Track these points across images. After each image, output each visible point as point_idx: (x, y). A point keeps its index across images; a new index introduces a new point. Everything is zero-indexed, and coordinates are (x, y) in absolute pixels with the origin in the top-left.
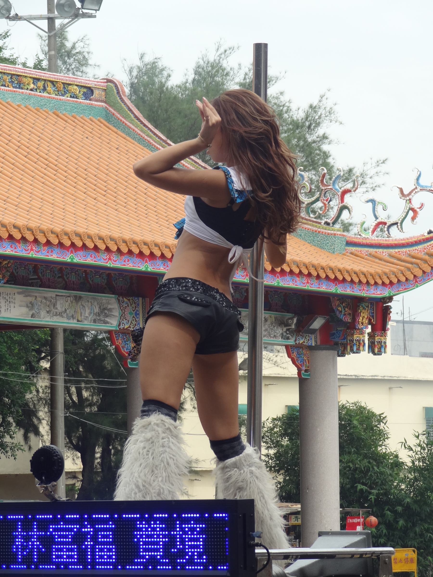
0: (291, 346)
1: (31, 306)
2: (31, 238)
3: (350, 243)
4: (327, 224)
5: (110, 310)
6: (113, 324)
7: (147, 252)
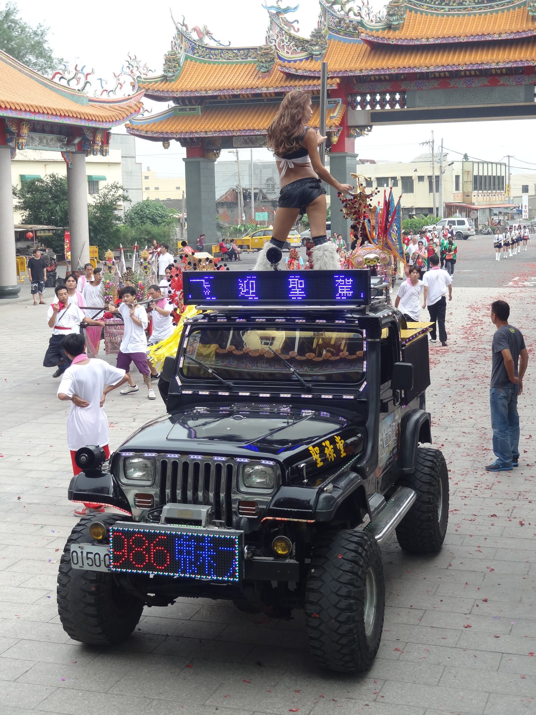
0: (64, 152)
3: (90, 101)
4: (79, 90)
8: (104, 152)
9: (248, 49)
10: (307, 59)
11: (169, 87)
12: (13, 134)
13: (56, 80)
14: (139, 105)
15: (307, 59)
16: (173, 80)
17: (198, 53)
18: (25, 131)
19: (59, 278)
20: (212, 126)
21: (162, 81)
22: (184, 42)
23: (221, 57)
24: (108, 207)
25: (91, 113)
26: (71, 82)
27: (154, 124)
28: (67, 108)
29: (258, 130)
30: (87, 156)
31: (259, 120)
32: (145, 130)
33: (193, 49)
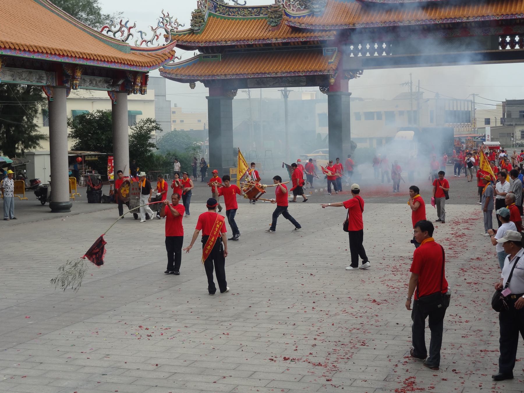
1: (12, 76)
2: (18, 48)
3: (132, 49)
4: (123, 41)
5: (43, 77)
6: (44, 83)
7: (62, 54)
8: (143, 92)
9: (261, 8)
10: (309, 15)
11: (196, 38)
12: (69, 76)
13: (104, 32)
14: (172, 53)
15: (309, 15)
16: (198, 33)
17: (219, 11)
18: (79, 74)
19: (104, 196)
20: (230, 70)
21: (190, 34)
22: (208, 2)
23: (238, 14)
24: (143, 136)
25: (132, 59)
26: (116, 35)
27: (183, 68)
28: (113, 56)
29: (269, 73)
30: (128, 94)
31: (269, 65)
32: (176, 73)
33: (215, 7)
